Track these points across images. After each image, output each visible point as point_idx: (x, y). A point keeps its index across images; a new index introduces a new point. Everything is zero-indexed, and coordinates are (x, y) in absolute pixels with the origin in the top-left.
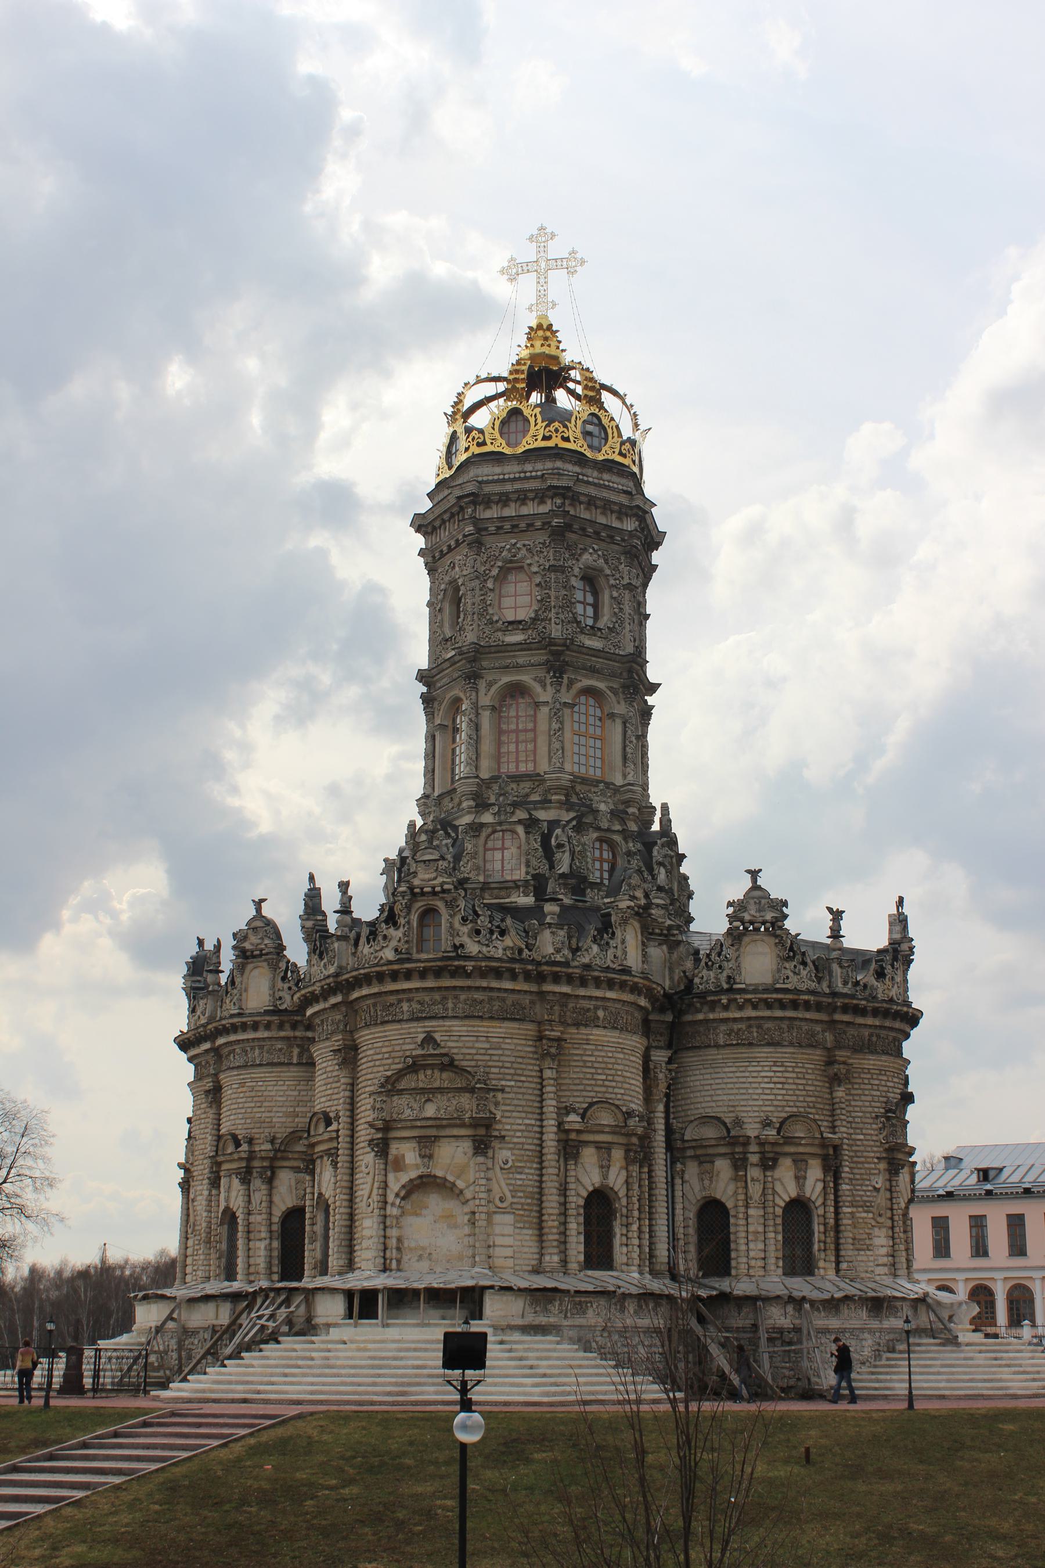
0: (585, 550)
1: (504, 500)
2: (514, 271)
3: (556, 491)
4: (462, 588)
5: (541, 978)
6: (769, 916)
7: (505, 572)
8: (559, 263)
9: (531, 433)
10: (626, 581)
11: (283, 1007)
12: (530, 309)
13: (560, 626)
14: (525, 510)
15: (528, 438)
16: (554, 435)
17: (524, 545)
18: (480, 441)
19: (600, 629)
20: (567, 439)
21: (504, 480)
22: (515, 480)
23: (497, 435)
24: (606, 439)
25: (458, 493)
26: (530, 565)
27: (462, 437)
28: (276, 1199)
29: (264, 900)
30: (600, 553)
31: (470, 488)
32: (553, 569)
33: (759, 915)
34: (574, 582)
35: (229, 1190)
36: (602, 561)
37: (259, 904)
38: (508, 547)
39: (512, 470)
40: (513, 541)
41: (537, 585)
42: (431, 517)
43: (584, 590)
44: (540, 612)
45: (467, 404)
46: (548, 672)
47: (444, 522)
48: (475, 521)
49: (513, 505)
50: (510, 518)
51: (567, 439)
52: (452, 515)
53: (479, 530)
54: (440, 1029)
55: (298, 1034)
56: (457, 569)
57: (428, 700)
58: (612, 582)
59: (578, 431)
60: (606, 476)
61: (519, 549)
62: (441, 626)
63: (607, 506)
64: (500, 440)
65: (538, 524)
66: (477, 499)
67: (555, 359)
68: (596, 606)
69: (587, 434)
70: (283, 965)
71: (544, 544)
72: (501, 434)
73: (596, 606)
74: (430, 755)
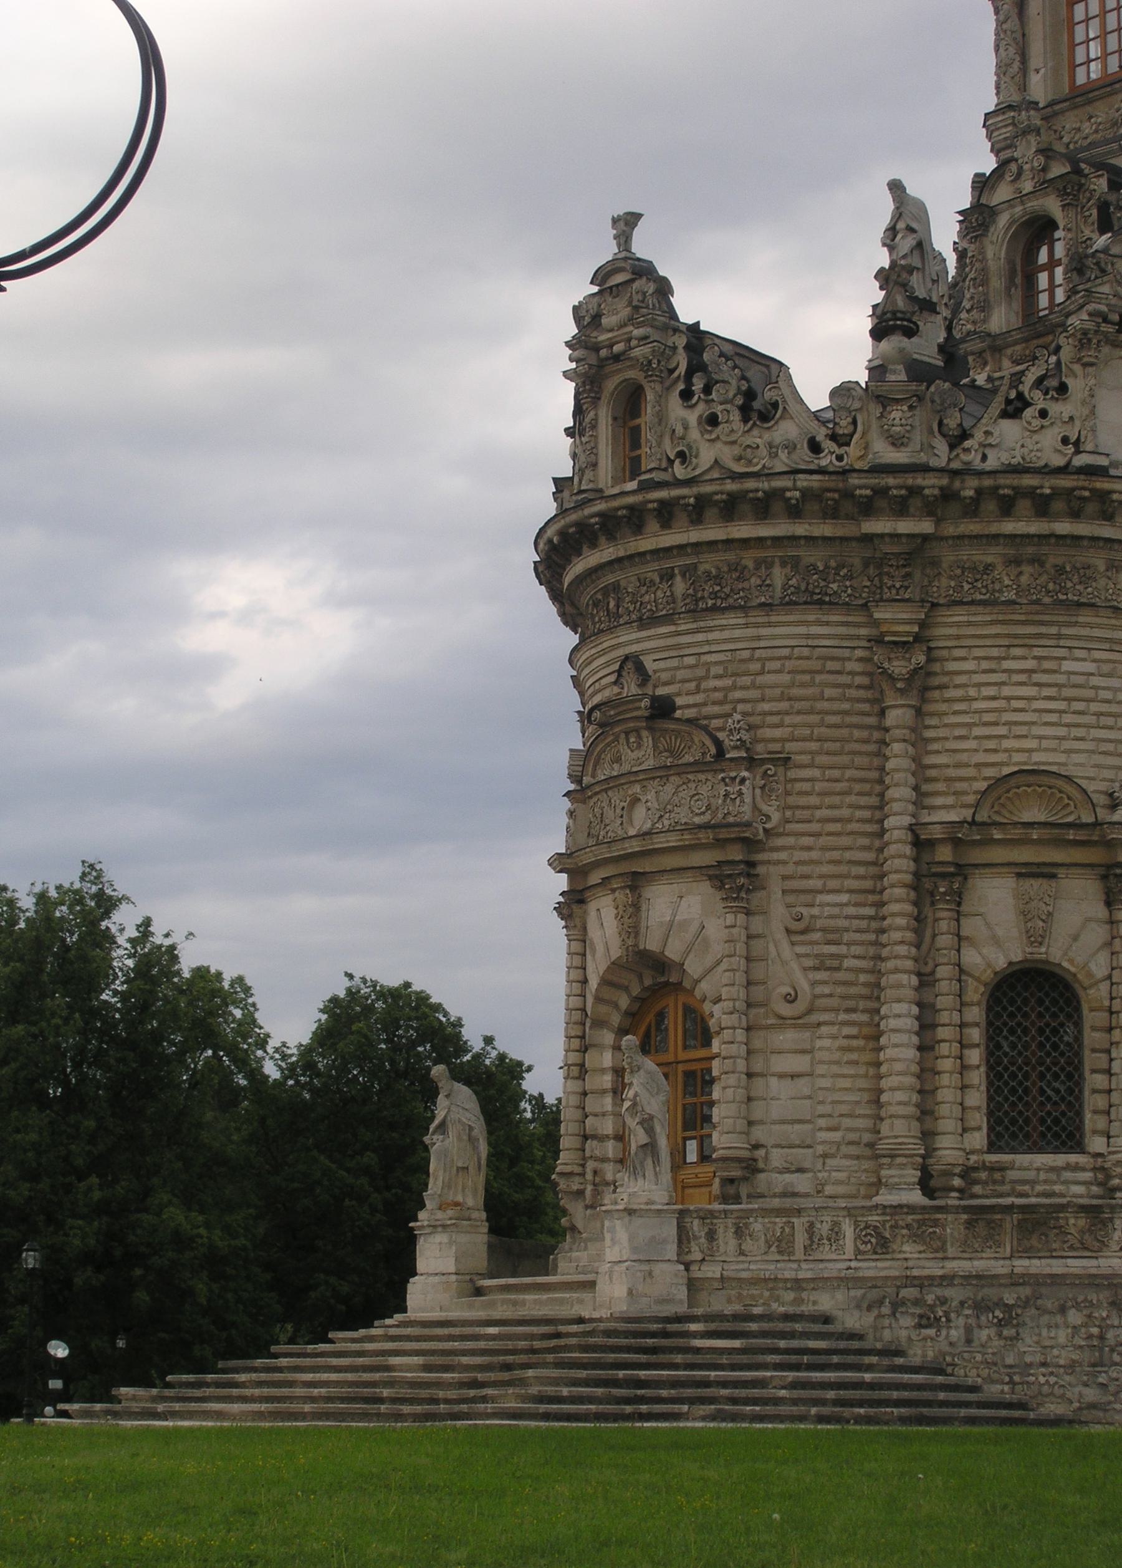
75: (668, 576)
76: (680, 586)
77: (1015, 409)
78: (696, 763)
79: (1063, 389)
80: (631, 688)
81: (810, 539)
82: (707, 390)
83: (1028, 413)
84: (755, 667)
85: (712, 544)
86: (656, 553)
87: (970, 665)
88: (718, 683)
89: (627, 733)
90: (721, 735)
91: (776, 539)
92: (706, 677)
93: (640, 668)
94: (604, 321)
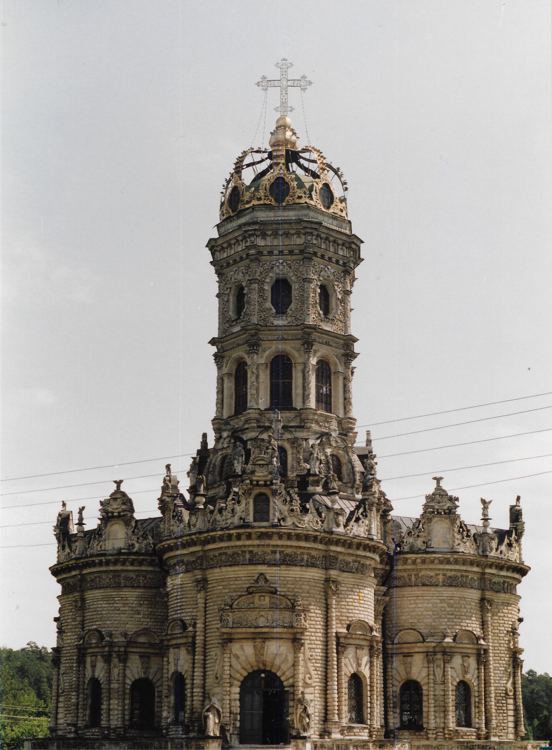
5: (330, 542)
6: (449, 504)
11: (135, 550)
28: (128, 672)
29: (121, 481)
33: (441, 506)
35: (94, 666)
37: (118, 483)
40: (281, 261)
46: (303, 345)
54: (269, 571)
55: (144, 568)
57: (218, 357)
62: (228, 311)
70: (133, 524)
74: (220, 391)
75: (274, 552)
76: (278, 556)
77: (357, 520)
78: (284, 608)
79: (366, 516)
80: (262, 583)
81: (316, 549)
82: (291, 501)
83: (360, 522)
84: (301, 583)
85: (291, 546)
86: (273, 546)
87: (345, 589)
88: (291, 586)
89: (260, 596)
90: (292, 601)
91: (309, 548)
92: (287, 584)
93: (265, 578)
94: (256, 474)
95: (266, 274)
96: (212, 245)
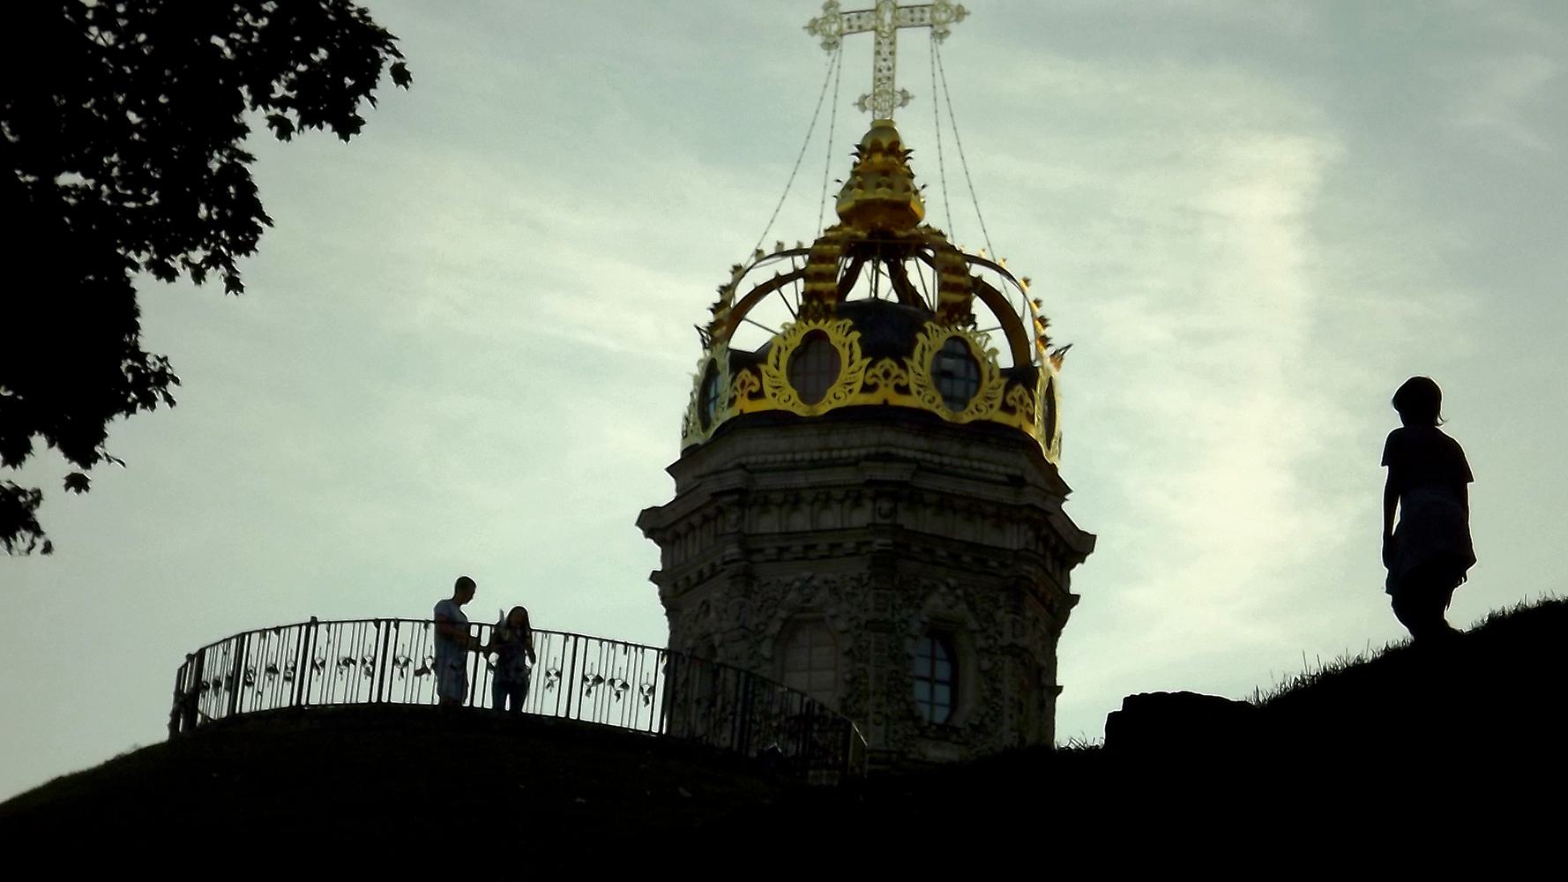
0: (935, 587)
1: (793, 500)
2: (835, 27)
3: (880, 489)
4: (720, 651)
7: (791, 627)
8: (917, 15)
9: (844, 375)
10: (1007, 639)
12: (861, 105)
13: (882, 729)
14: (830, 519)
15: (836, 388)
16: (882, 382)
17: (826, 582)
18: (754, 389)
19: (956, 730)
20: (903, 390)
21: (794, 467)
22: (815, 465)
23: (783, 378)
24: (979, 382)
25: (712, 486)
26: (834, 617)
27: (725, 377)
30: (959, 592)
31: (734, 480)
32: (873, 625)
34: (909, 647)
36: (963, 606)
38: (797, 584)
39: (805, 445)
41: (849, 653)
42: (671, 518)
43: (933, 658)
44: (850, 702)
45: (742, 291)
47: (692, 527)
48: (743, 540)
49: (806, 508)
50: (803, 534)
51: (903, 390)
52: (706, 519)
53: (748, 552)
56: (713, 615)
58: (981, 643)
59: (926, 372)
60: (976, 451)
61: (816, 588)
63: (972, 509)
64: (790, 391)
65: (850, 545)
66: (746, 499)
67: (904, 210)
68: (954, 684)
69: (940, 375)
71: (859, 580)
72: (792, 374)
73: (954, 684)
95: (771, 612)
96: (652, 522)
